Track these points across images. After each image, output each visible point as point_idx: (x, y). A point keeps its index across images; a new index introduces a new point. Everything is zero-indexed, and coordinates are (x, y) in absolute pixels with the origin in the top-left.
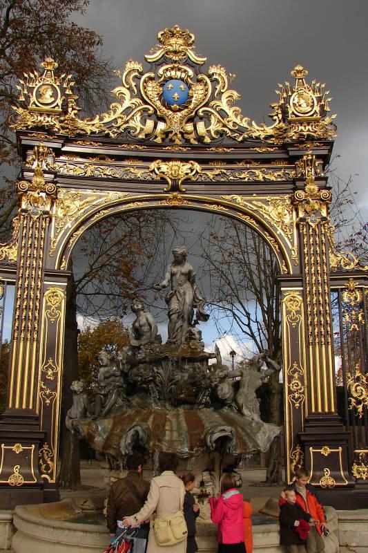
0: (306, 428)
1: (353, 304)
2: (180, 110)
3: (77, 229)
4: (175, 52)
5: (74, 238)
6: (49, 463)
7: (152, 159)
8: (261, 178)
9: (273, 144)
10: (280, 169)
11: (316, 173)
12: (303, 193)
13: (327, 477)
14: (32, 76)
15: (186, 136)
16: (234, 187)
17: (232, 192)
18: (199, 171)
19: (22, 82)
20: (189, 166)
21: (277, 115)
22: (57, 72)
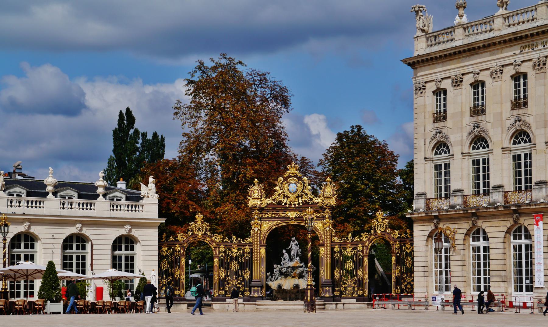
1: (337, 251)
3: (267, 232)
4: (293, 173)
7: (286, 212)
10: (320, 213)
19: (249, 189)
22: (259, 183)
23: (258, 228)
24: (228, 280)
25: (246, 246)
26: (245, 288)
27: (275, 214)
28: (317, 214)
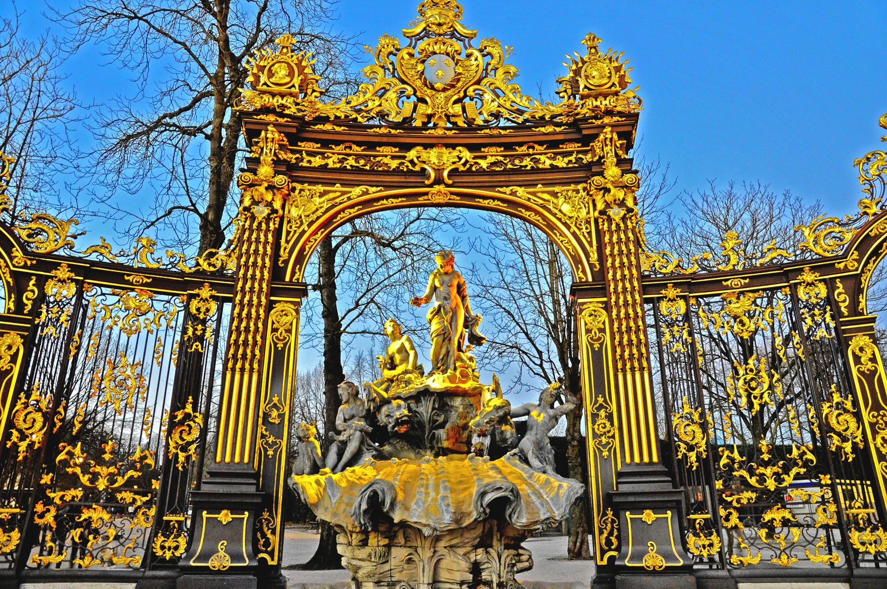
0: (619, 485)
2: (444, 90)
5: (311, 244)
6: (269, 536)
7: (408, 147)
8: (547, 165)
9: (562, 122)
10: (570, 153)
11: (617, 155)
12: (602, 179)
13: (652, 553)
14: (264, 53)
15: (453, 119)
16: (514, 178)
17: (511, 184)
18: (468, 159)
20: (455, 153)
21: (565, 91)
23: (269, 204)
24: (65, 463)
25: (200, 285)
26: (160, 514)
27: (358, 157)
28: (554, 159)
